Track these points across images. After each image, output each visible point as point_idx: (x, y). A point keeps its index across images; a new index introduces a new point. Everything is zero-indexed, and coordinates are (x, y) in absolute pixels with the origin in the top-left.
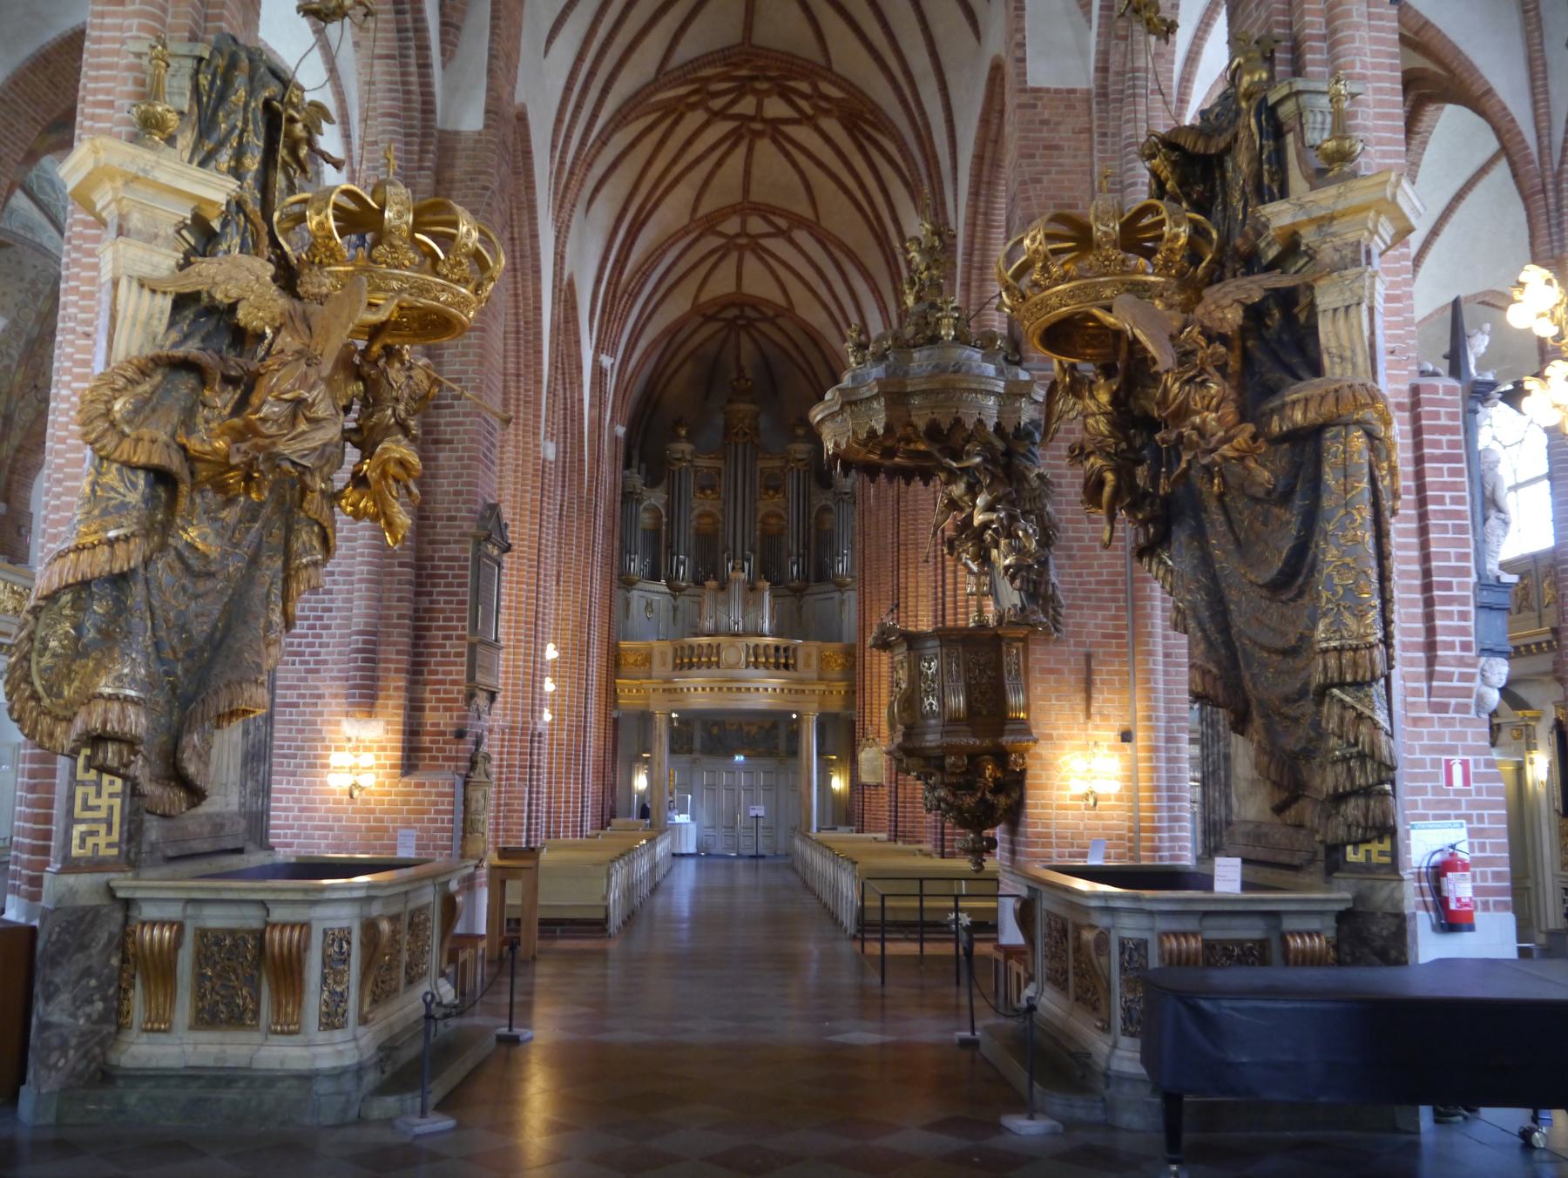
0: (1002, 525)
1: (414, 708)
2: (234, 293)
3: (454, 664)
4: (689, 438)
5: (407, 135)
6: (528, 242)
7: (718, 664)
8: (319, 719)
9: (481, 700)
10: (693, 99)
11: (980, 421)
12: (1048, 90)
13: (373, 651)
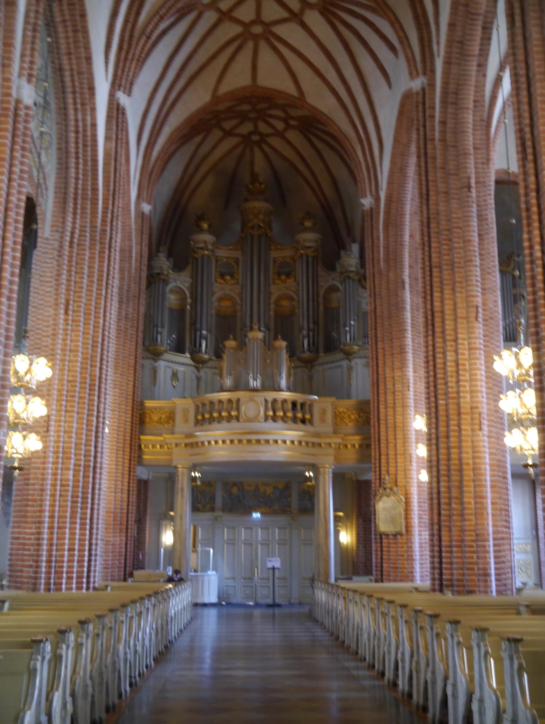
4: (211, 230)
7: (237, 418)
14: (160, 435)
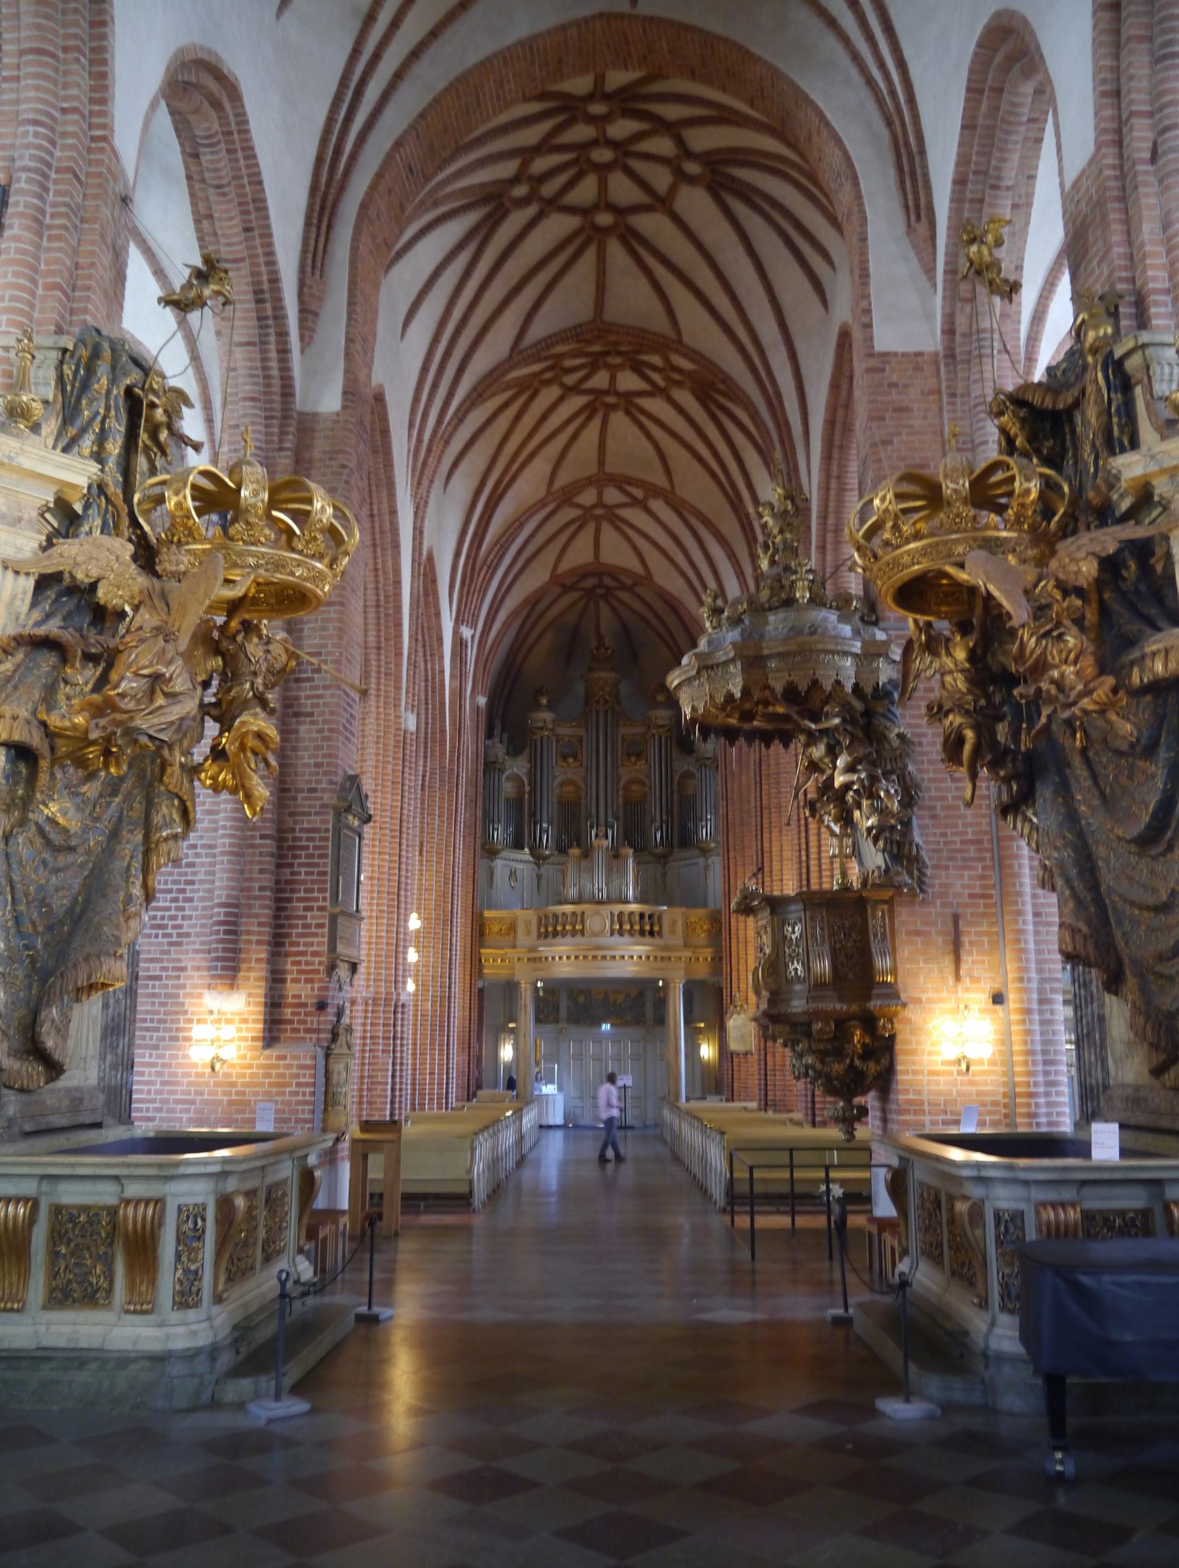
0: (863, 787)
1: (276, 979)
2: (95, 573)
3: (316, 935)
4: (550, 707)
5: (267, 418)
6: (387, 517)
8: (181, 992)
9: (343, 971)
10: (547, 375)
11: (838, 682)
12: (895, 354)
13: (235, 923)
14: (501, 948)
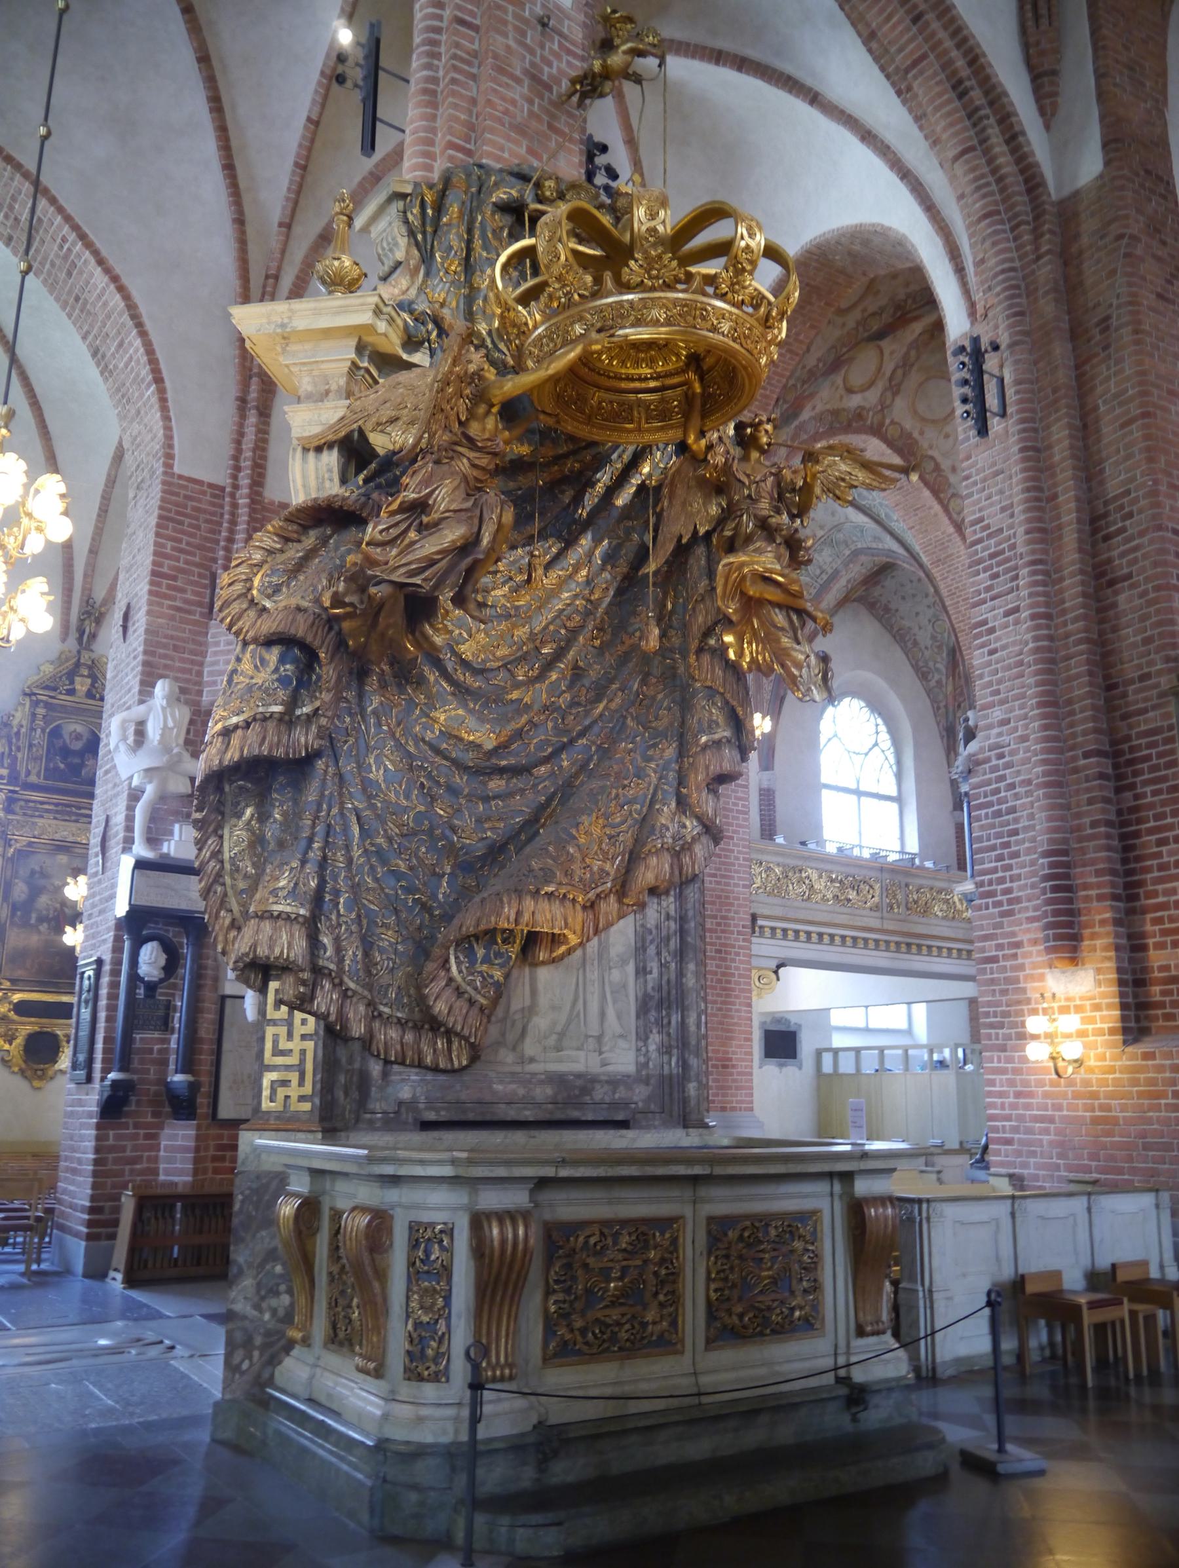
8: (1021, 974)
13: (1067, 876)
